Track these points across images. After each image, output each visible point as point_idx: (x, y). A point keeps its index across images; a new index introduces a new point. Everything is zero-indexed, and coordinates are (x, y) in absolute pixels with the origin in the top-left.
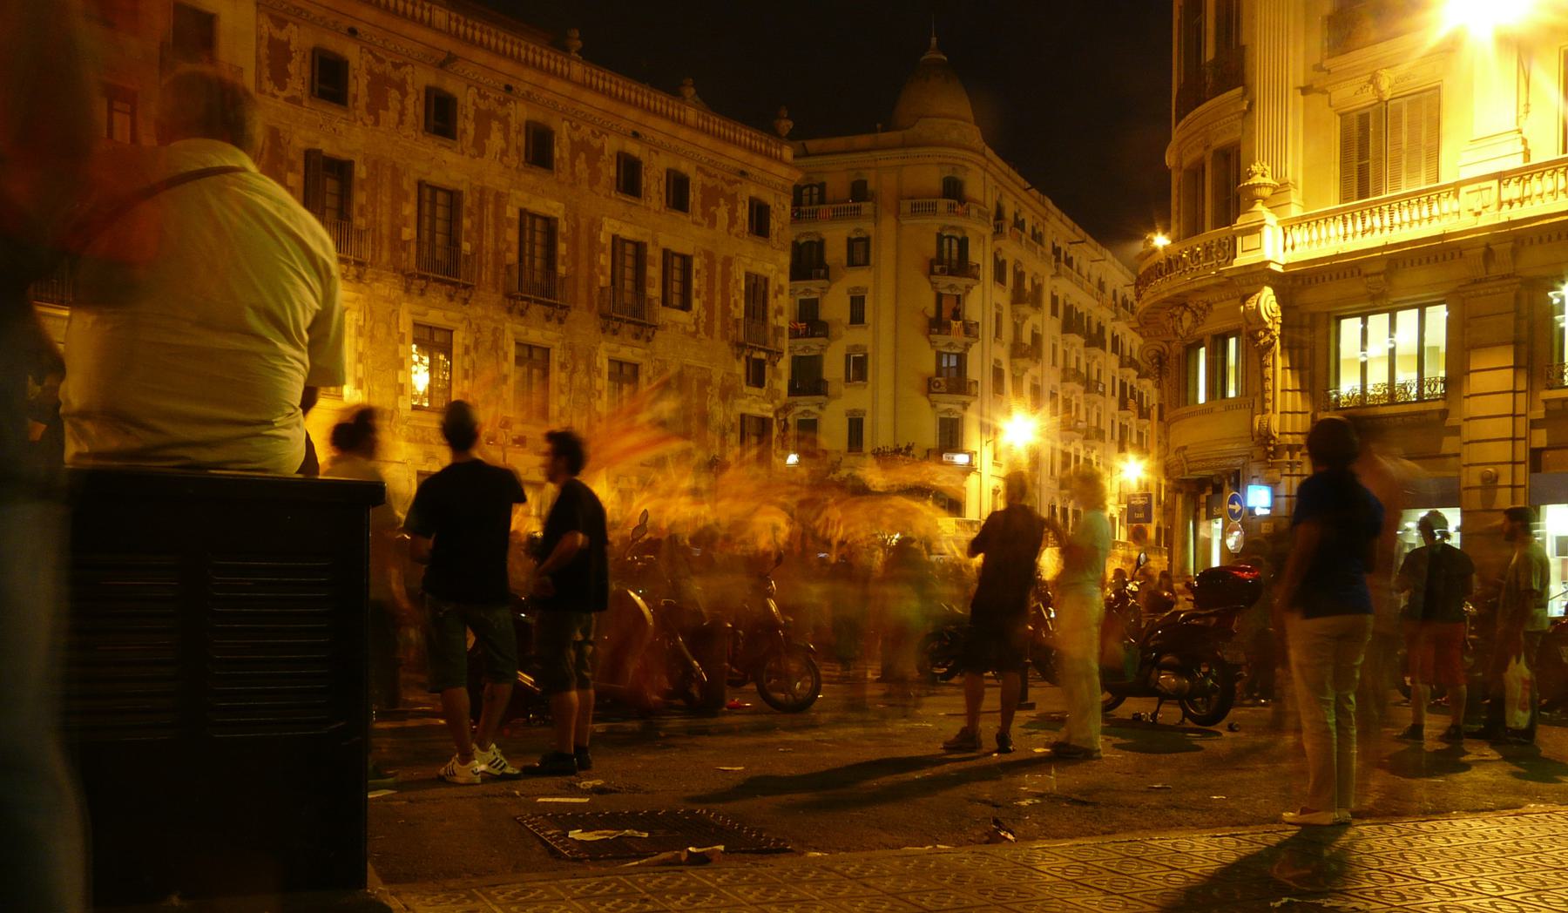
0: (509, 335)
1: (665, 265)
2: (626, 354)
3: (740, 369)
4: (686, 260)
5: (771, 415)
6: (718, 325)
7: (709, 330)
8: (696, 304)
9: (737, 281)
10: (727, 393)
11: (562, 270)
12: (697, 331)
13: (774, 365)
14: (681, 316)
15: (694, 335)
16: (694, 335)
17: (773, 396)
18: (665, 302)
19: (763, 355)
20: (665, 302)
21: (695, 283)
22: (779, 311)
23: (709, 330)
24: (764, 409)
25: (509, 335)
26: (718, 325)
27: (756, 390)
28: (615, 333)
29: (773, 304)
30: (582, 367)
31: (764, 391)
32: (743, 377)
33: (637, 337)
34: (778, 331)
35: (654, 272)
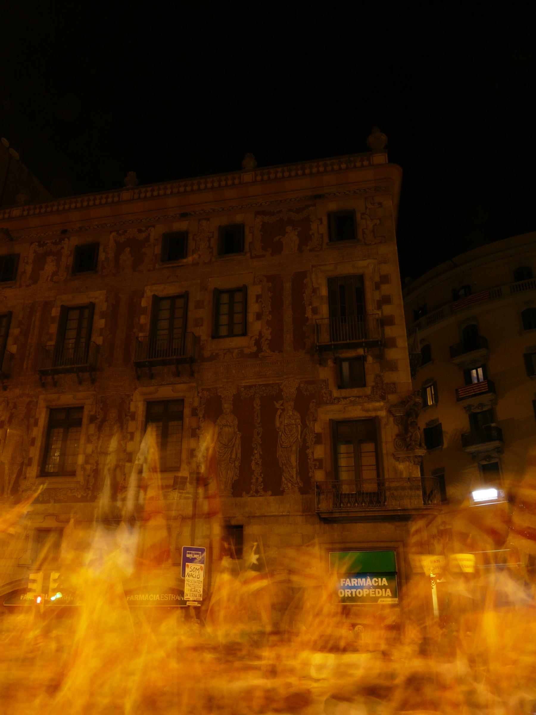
0: (42, 404)
1: (217, 304)
2: (166, 392)
3: (325, 373)
4: (243, 290)
5: (383, 413)
6: (288, 338)
7: (276, 344)
8: (256, 327)
9: (315, 290)
10: (304, 404)
11: (97, 339)
12: (260, 350)
13: (380, 358)
14: (236, 342)
15: (254, 355)
16: (254, 355)
17: (383, 391)
18: (215, 335)
19: (361, 351)
20: (215, 335)
21: (254, 308)
22: (386, 300)
23: (276, 344)
24: (378, 409)
25: (42, 404)
26: (288, 338)
27: (355, 391)
28: (152, 377)
29: (371, 296)
30: (113, 414)
31: (368, 390)
32: (331, 381)
33: (178, 374)
34: (386, 321)
35: (200, 314)
